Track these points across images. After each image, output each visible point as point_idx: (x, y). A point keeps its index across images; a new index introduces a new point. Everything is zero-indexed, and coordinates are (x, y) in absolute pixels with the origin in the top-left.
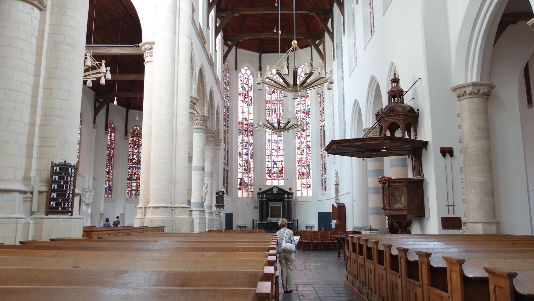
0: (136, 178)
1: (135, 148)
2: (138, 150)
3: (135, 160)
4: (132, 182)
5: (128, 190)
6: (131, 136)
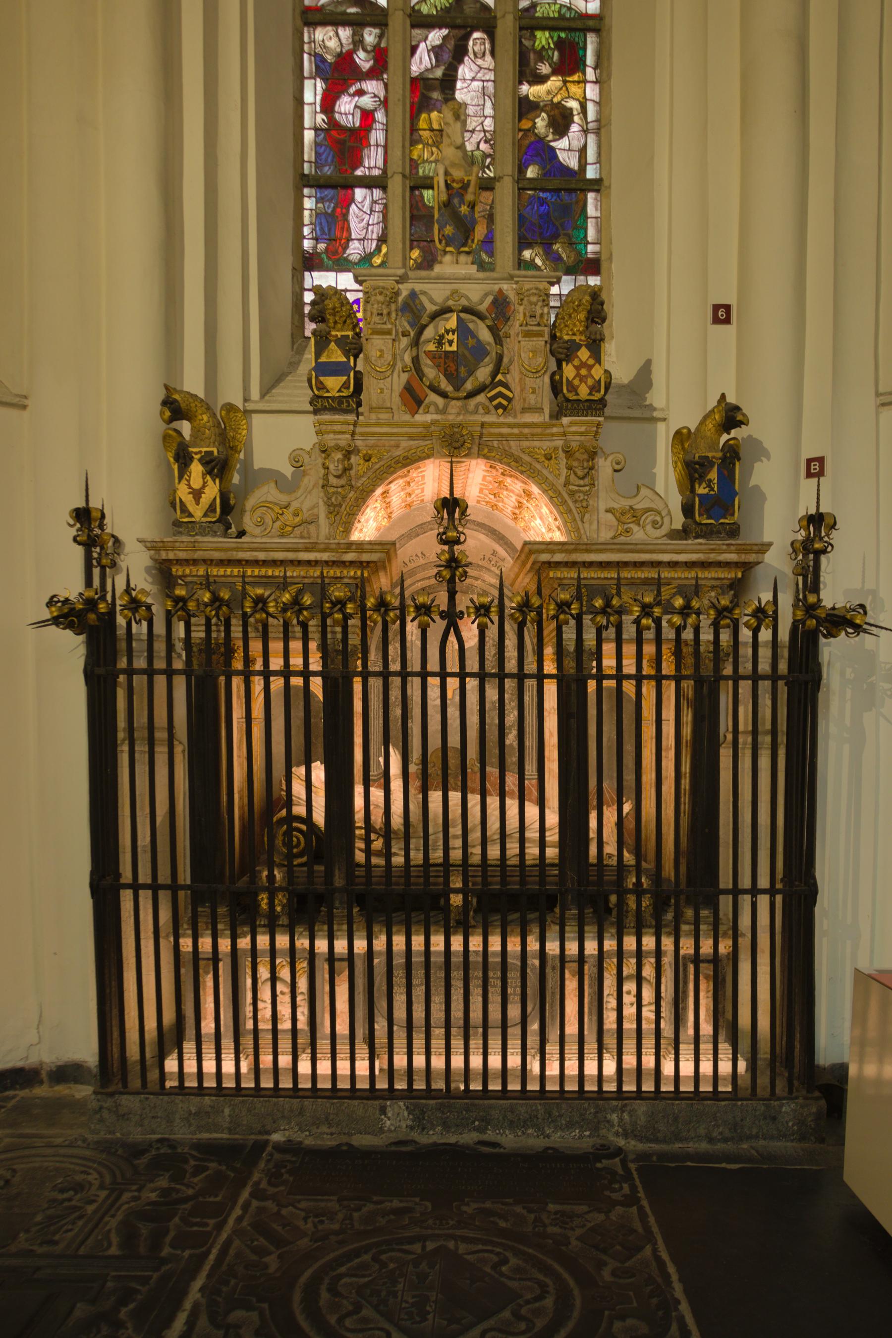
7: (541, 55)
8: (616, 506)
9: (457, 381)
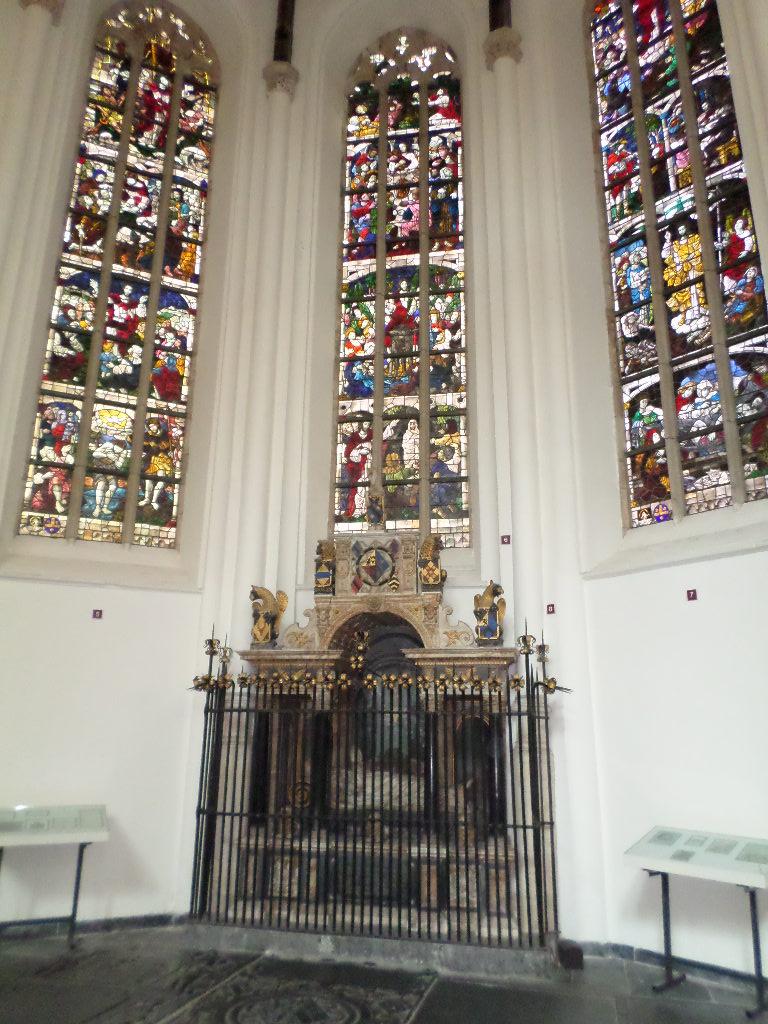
0: (136, 368)
1: (142, 142)
2: (170, 164)
3: (133, 226)
4: (90, 400)
5: (48, 466)
6: (114, 56)
7: (440, 426)
8: (448, 630)
9: (375, 578)
